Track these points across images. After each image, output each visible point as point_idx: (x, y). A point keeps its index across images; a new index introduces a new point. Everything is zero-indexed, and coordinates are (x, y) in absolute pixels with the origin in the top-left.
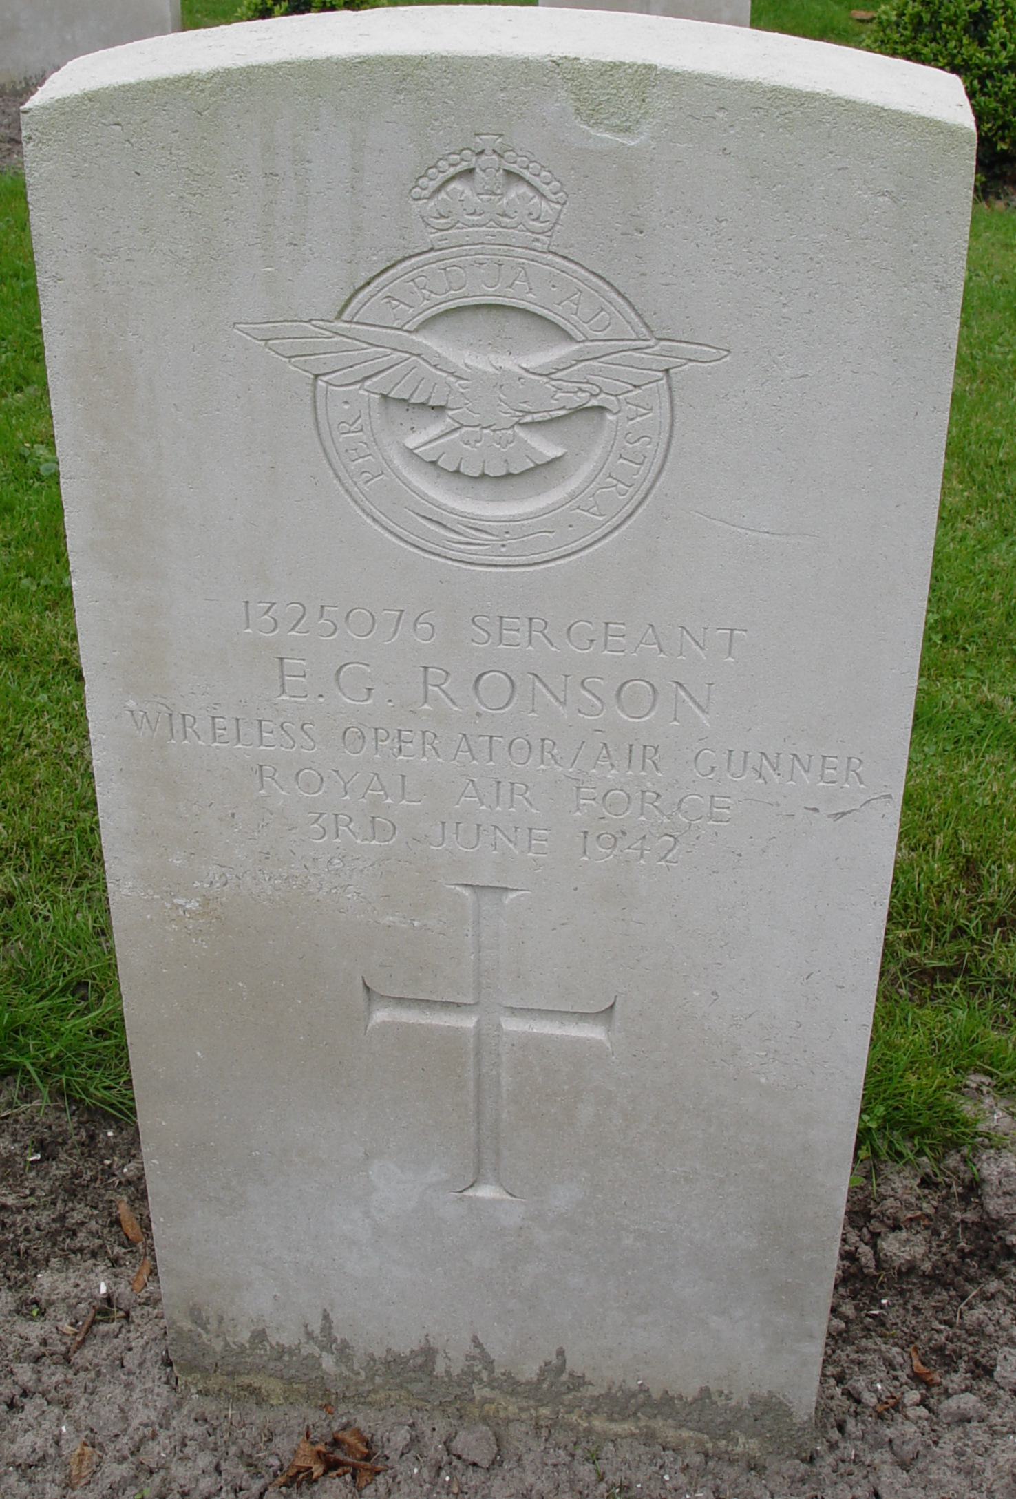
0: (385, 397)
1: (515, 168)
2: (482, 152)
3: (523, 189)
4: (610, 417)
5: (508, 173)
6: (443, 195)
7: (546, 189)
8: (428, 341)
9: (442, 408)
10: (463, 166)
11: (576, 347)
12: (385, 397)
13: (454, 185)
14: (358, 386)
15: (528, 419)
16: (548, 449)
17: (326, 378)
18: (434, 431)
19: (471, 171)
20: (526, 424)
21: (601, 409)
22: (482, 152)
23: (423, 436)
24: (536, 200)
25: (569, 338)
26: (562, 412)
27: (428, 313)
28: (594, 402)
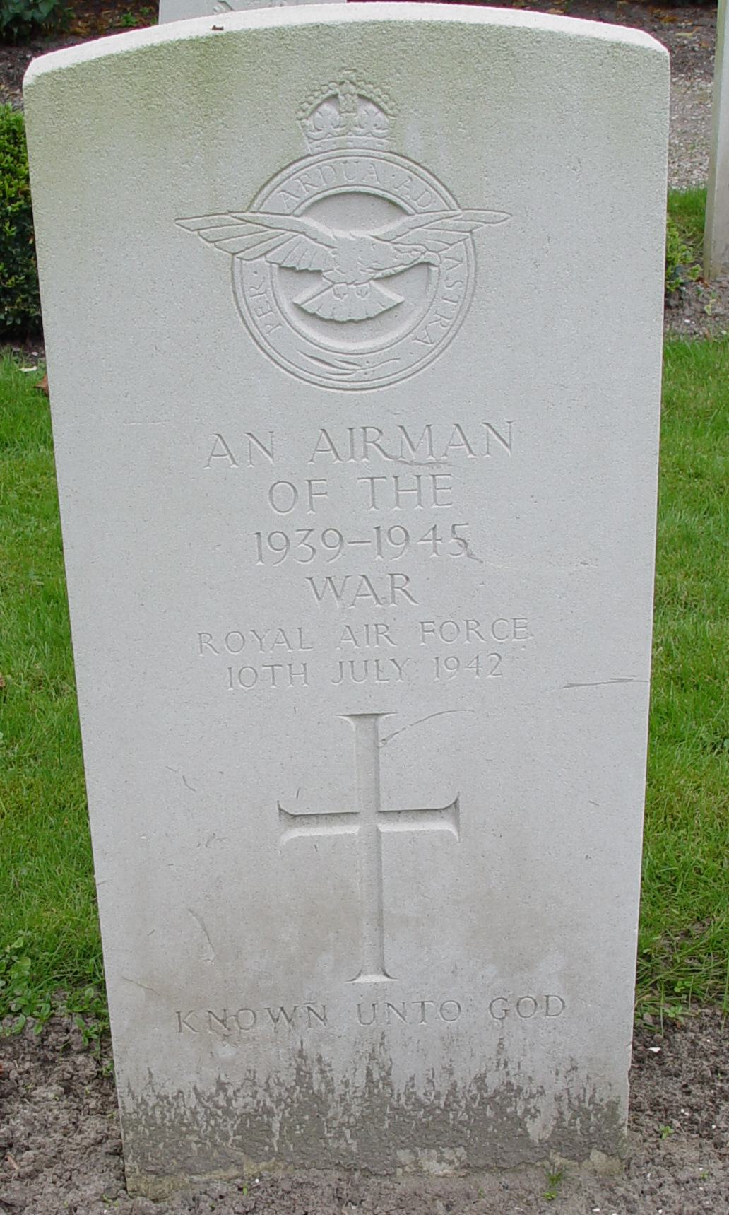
0: (281, 268)
1: (363, 92)
2: (342, 83)
3: (371, 107)
4: (433, 269)
5: (360, 96)
6: (317, 115)
7: (386, 107)
8: (308, 221)
9: (319, 272)
10: (330, 92)
11: (406, 219)
12: (281, 268)
13: (325, 107)
14: (263, 259)
15: (379, 274)
16: (391, 295)
17: (240, 255)
18: (316, 286)
19: (335, 96)
20: (377, 279)
21: (428, 264)
22: (342, 83)
23: (306, 293)
24: (380, 115)
25: (405, 212)
26: (402, 267)
27: (312, 200)
28: (422, 259)
